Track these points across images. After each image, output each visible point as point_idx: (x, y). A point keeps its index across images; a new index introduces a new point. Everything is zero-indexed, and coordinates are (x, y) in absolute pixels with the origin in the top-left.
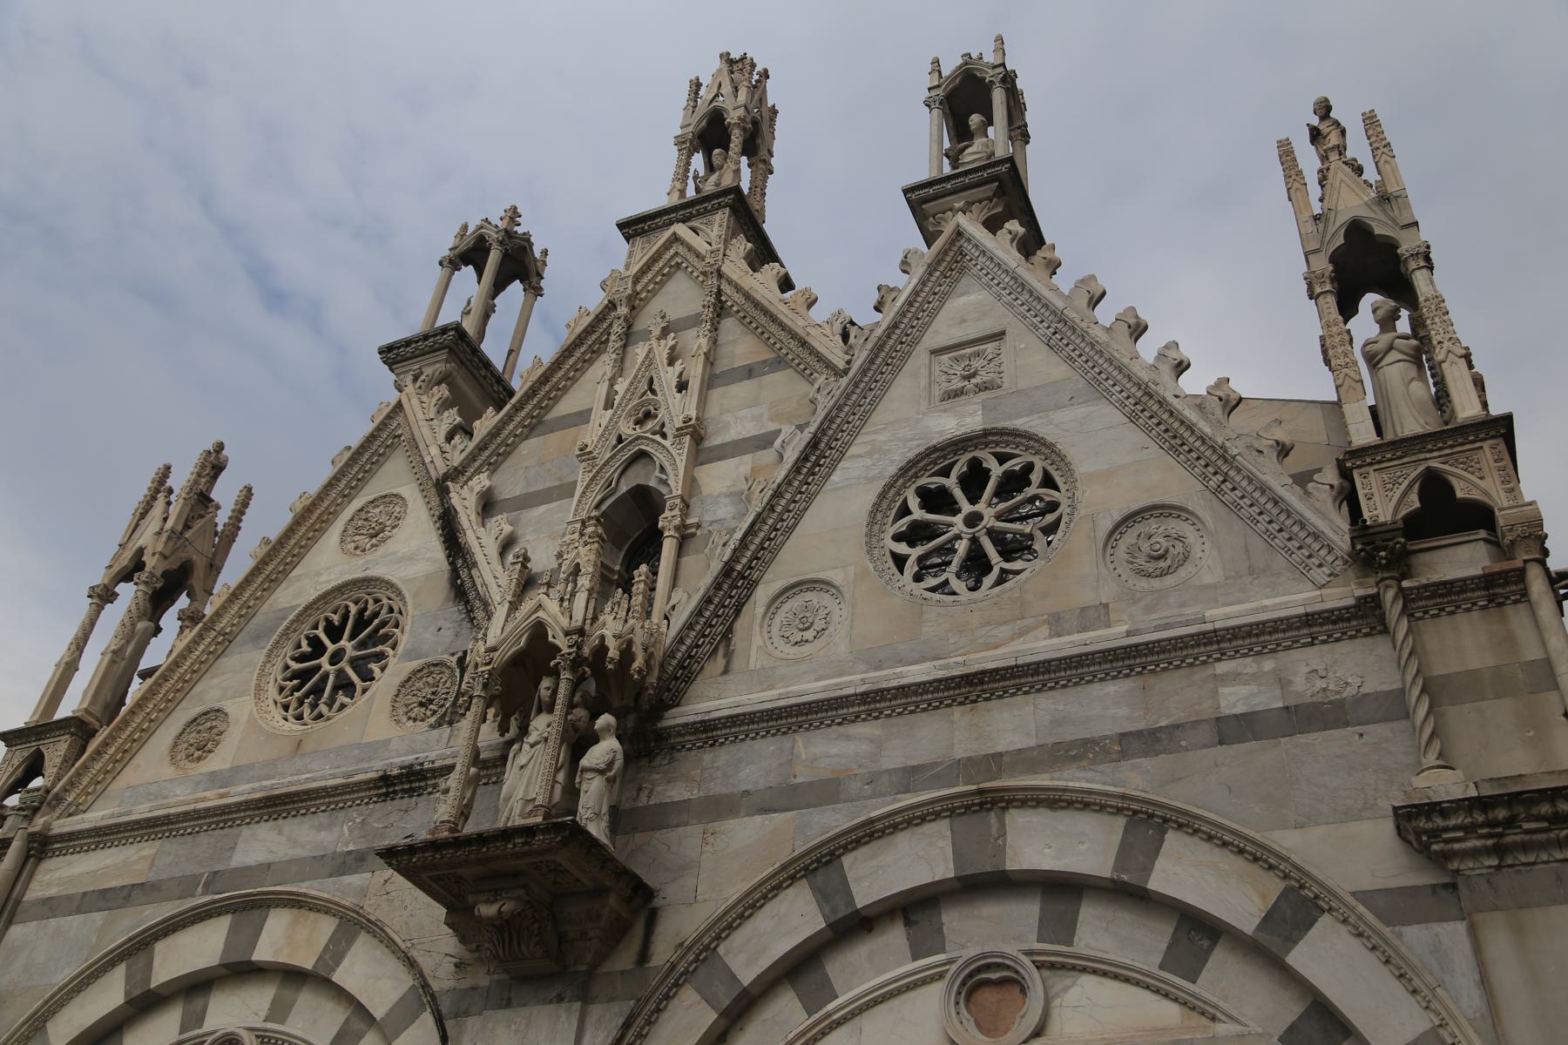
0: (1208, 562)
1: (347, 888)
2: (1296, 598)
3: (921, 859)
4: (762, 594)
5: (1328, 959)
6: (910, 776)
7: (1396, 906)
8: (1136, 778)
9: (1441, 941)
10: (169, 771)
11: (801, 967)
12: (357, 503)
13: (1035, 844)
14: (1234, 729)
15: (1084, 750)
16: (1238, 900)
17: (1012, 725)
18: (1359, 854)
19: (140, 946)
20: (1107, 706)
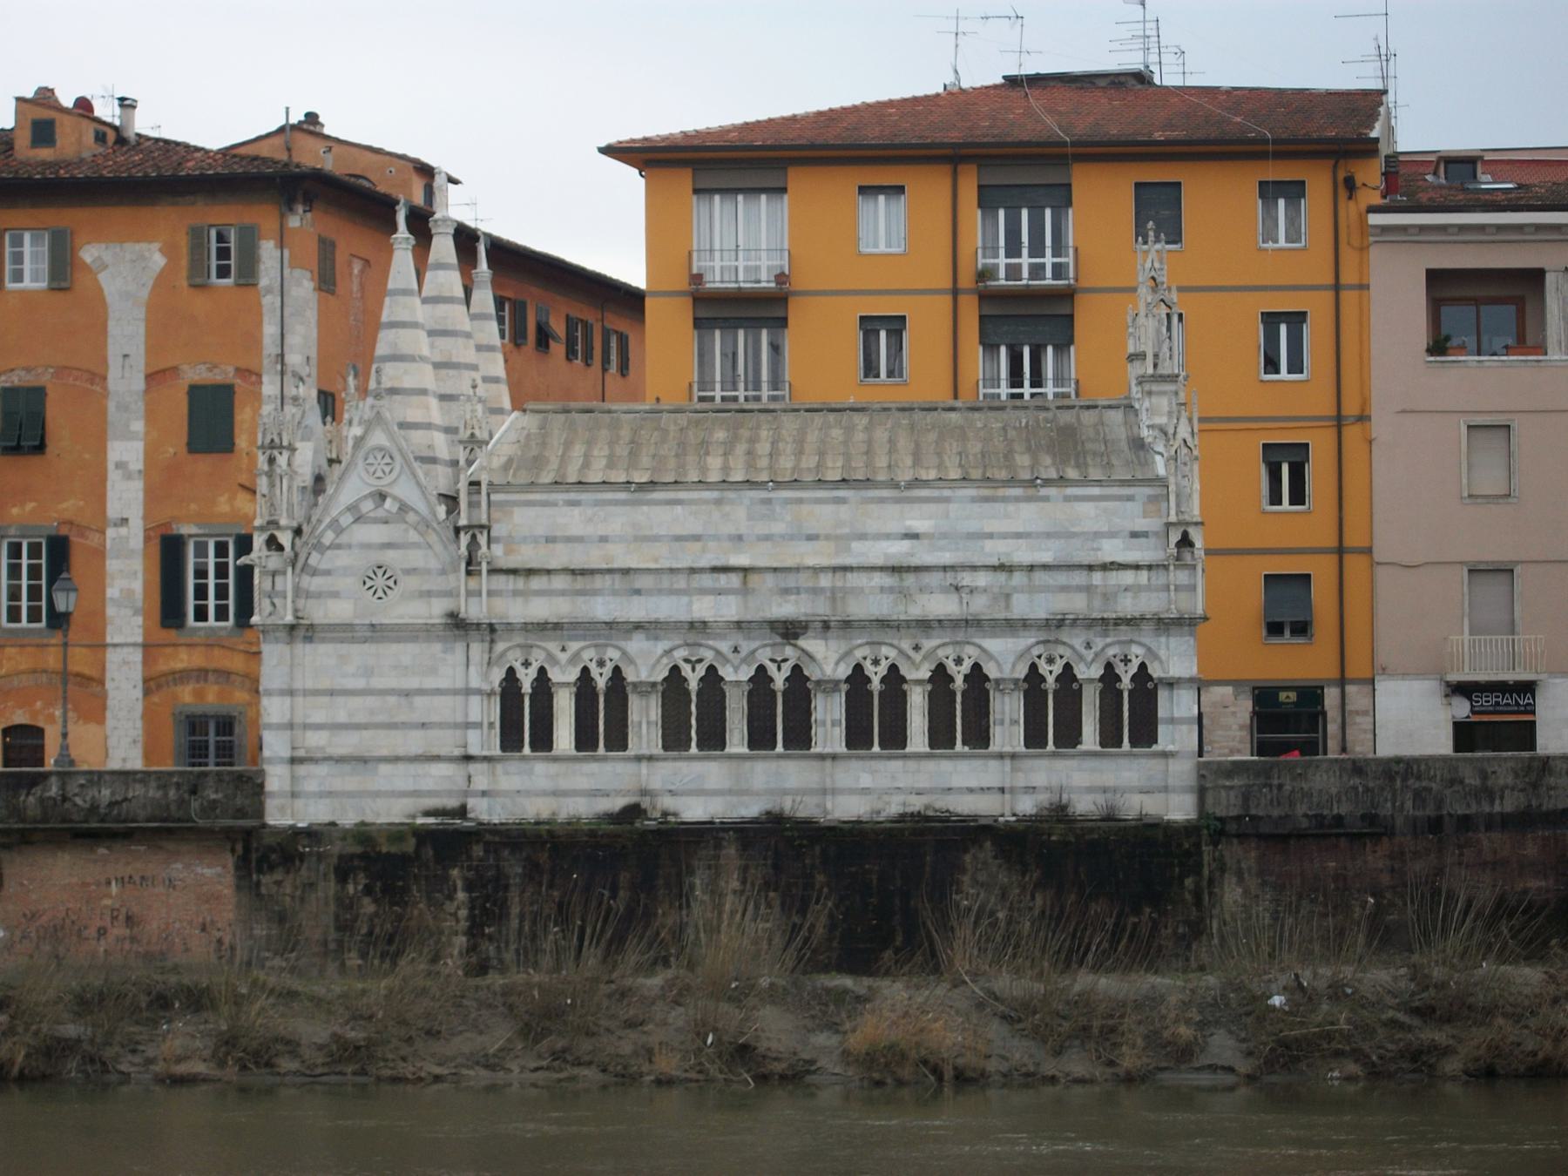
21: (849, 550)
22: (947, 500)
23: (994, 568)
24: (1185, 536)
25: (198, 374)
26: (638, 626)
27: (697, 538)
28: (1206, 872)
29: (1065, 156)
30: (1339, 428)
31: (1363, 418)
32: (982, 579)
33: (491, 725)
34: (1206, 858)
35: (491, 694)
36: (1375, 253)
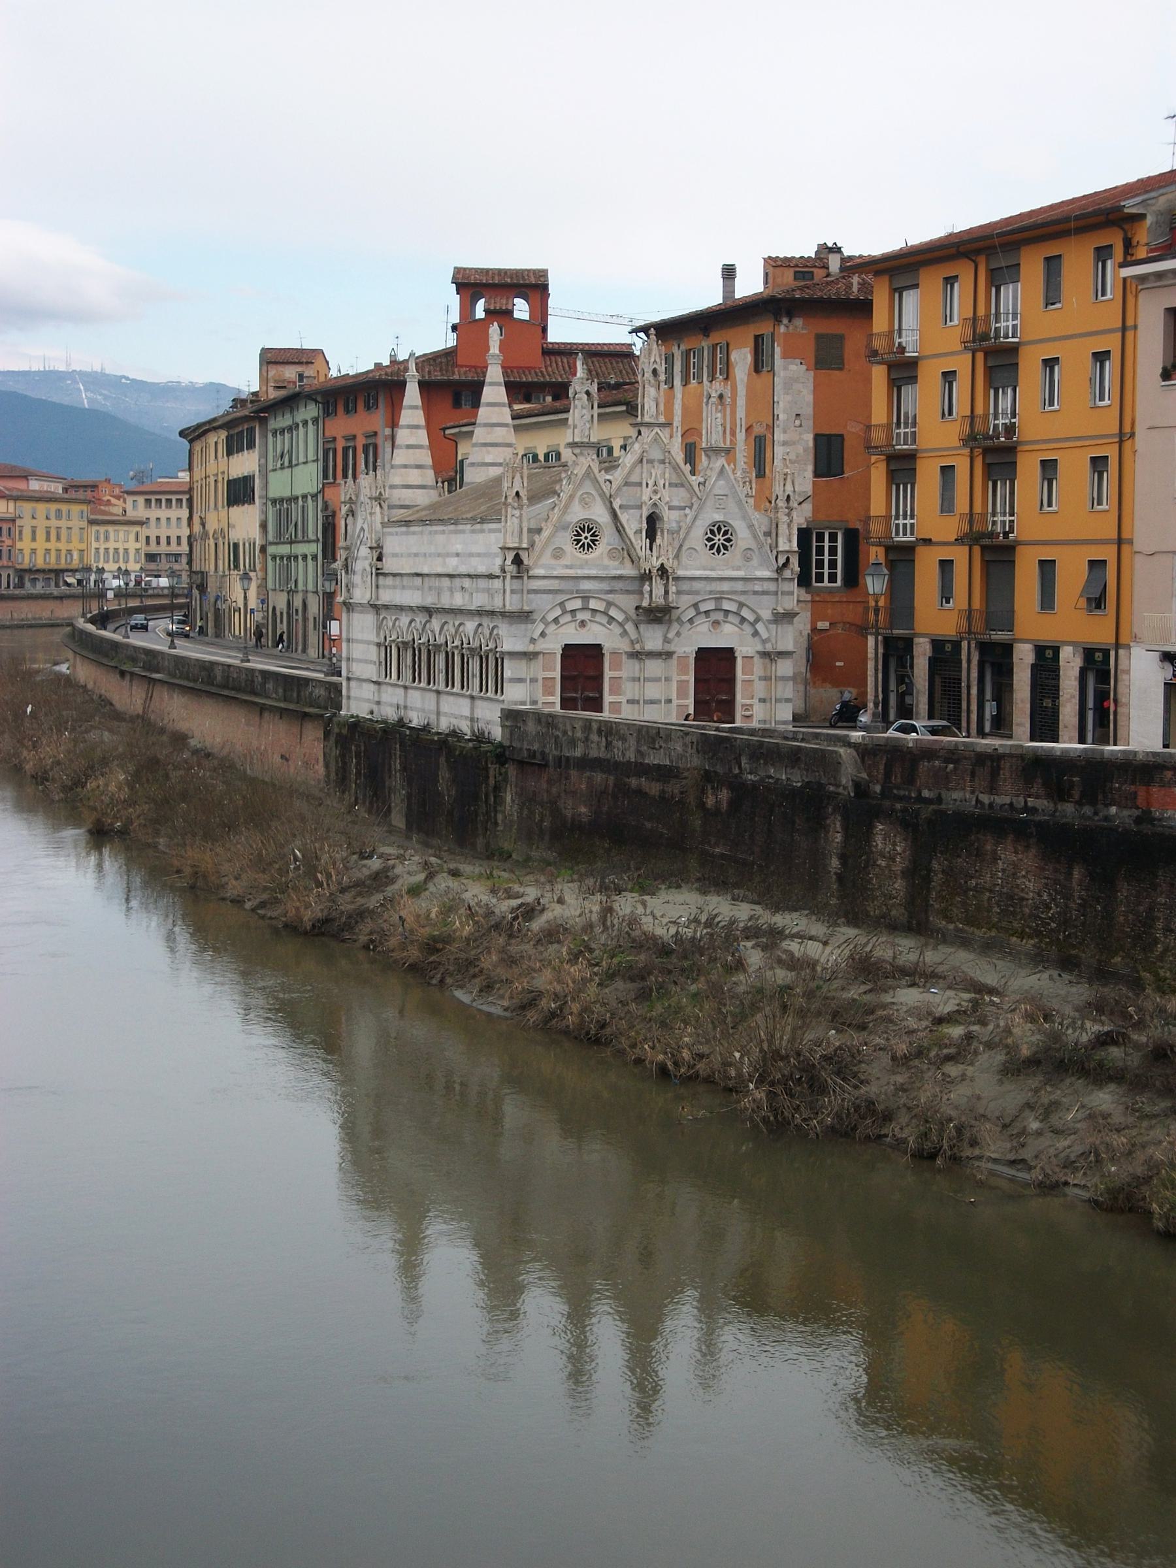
0: (755, 562)
1: (610, 597)
2: (767, 574)
3: (710, 605)
4: (684, 548)
5: (760, 627)
6: (711, 592)
7: (770, 622)
8: (742, 599)
9: (773, 627)
10: (553, 562)
11: (691, 621)
12: (580, 493)
13: (726, 605)
14: (755, 593)
15: (734, 592)
16: (751, 618)
17: (726, 586)
18: (766, 614)
19: (562, 604)
20: (739, 586)
21: (445, 563)
22: (463, 532)
23: (469, 576)
24: (517, 555)
25: (758, 430)
26: (401, 608)
27: (416, 555)
28: (492, 781)
29: (994, 247)
30: (1121, 442)
31: (1132, 435)
32: (467, 583)
33: (380, 663)
34: (491, 773)
35: (379, 645)
36: (1141, 296)
